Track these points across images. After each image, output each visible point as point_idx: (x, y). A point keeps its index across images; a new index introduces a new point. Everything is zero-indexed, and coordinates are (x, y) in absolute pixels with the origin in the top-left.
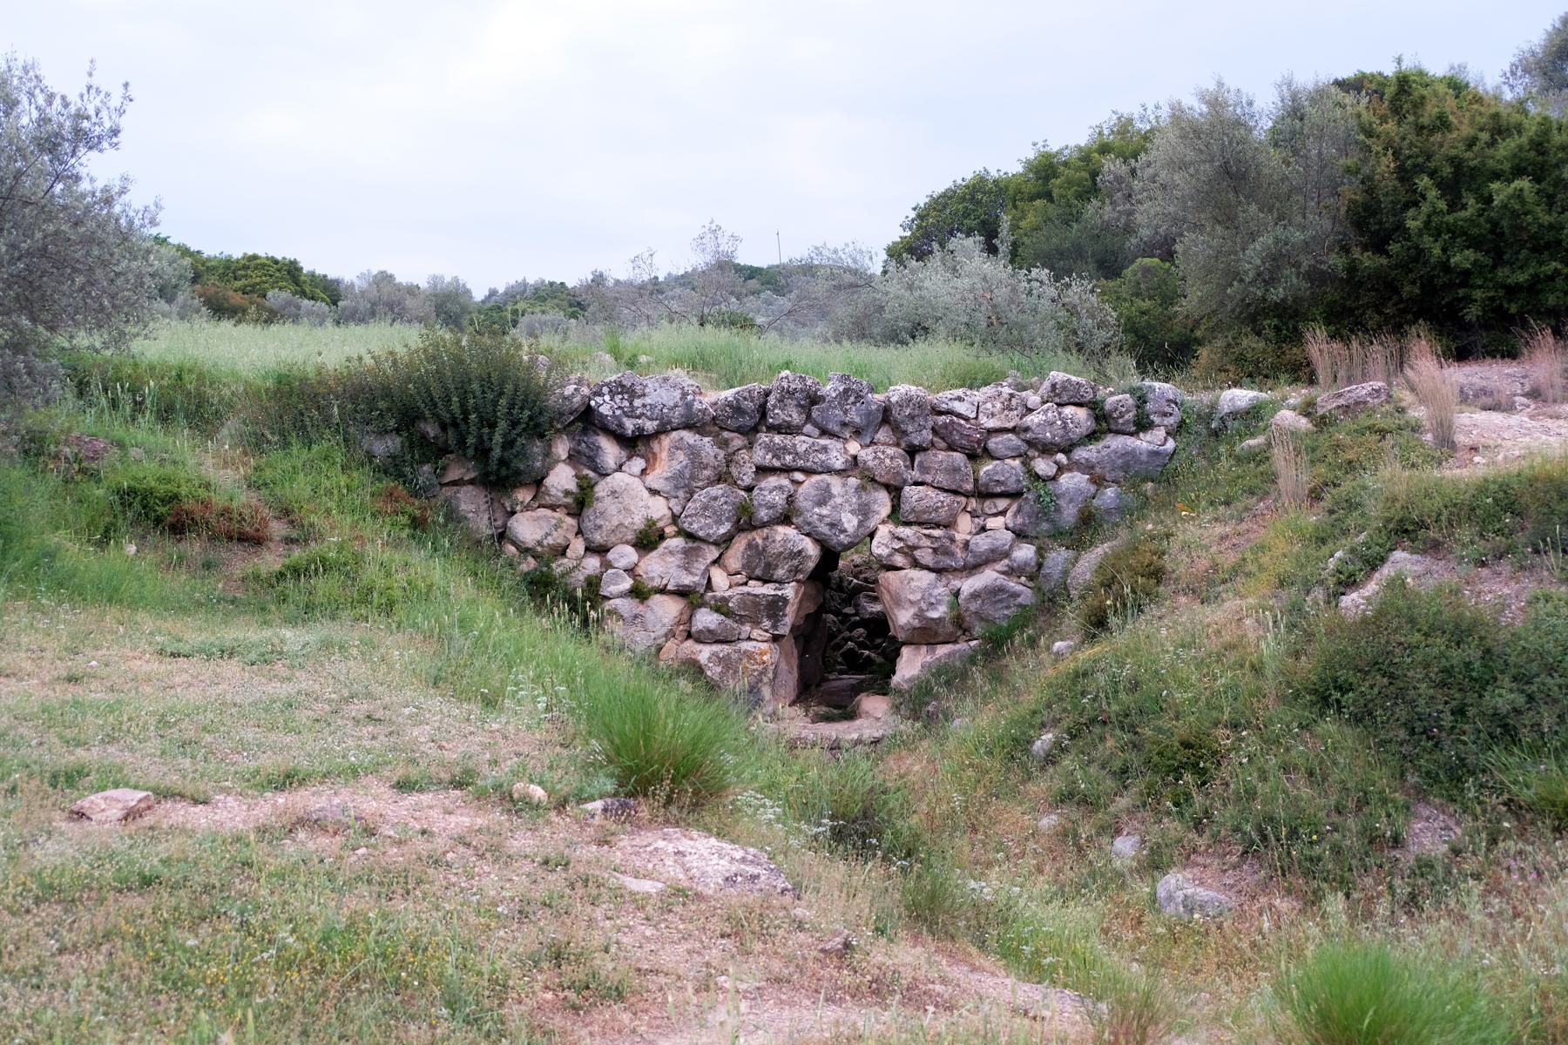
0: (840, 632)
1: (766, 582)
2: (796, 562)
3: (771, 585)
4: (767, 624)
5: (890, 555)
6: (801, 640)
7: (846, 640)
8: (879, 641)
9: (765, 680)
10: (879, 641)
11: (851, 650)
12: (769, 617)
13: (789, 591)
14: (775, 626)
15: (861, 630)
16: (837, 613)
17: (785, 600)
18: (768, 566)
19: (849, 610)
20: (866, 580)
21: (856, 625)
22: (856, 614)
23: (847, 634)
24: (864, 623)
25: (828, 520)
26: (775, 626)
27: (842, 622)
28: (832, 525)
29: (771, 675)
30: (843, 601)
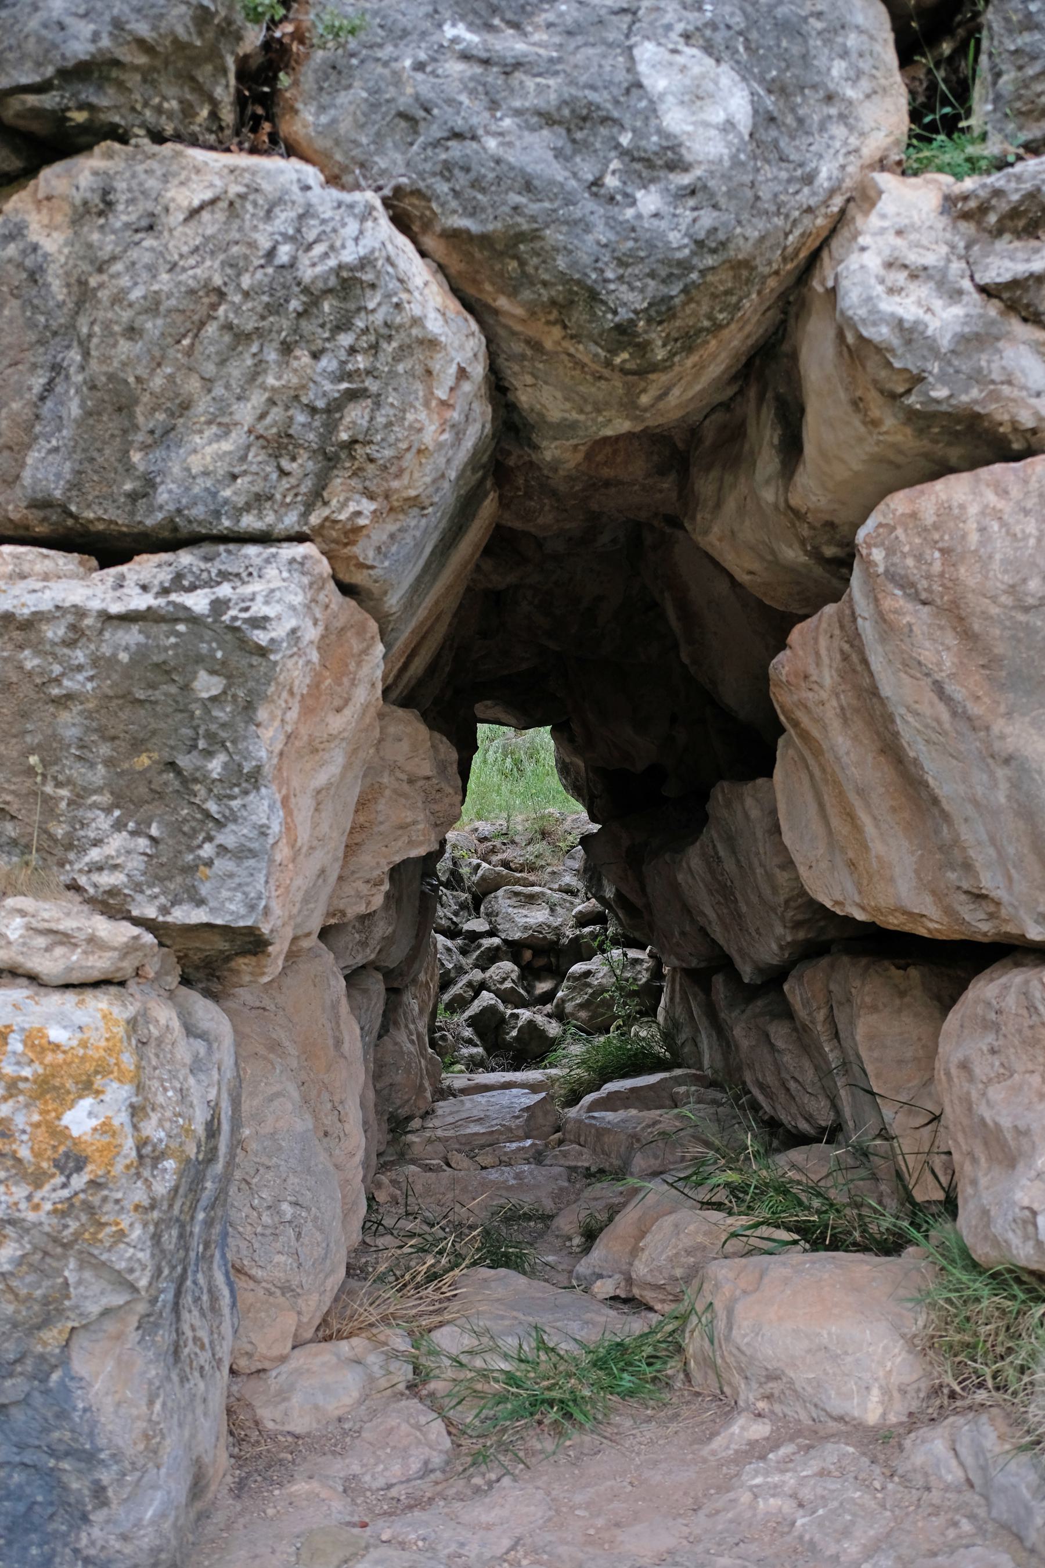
0: (460, 970)
1: (108, 550)
2: (319, 375)
3: (147, 567)
4: (116, 851)
5: (976, 340)
6: (377, 985)
7: (479, 988)
8: (543, 987)
9: (93, 1296)
10: (543, 987)
11: (489, 1011)
12: (130, 802)
13: (278, 593)
14: (176, 870)
15: (507, 966)
16: (452, 933)
17: (240, 649)
18: (116, 401)
19: (478, 925)
20: (505, 864)
21: (492, 957)
22: (492, 933)
23: (477, 975)
24: (513, 949)
25: (549, 91)
26: (176, 870)
27: (464, 952)
28: (577, 122)
29: (134, 1251)
30: (463, 906)
